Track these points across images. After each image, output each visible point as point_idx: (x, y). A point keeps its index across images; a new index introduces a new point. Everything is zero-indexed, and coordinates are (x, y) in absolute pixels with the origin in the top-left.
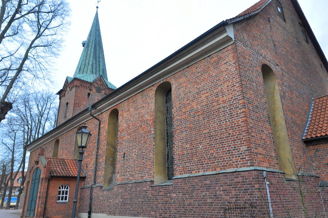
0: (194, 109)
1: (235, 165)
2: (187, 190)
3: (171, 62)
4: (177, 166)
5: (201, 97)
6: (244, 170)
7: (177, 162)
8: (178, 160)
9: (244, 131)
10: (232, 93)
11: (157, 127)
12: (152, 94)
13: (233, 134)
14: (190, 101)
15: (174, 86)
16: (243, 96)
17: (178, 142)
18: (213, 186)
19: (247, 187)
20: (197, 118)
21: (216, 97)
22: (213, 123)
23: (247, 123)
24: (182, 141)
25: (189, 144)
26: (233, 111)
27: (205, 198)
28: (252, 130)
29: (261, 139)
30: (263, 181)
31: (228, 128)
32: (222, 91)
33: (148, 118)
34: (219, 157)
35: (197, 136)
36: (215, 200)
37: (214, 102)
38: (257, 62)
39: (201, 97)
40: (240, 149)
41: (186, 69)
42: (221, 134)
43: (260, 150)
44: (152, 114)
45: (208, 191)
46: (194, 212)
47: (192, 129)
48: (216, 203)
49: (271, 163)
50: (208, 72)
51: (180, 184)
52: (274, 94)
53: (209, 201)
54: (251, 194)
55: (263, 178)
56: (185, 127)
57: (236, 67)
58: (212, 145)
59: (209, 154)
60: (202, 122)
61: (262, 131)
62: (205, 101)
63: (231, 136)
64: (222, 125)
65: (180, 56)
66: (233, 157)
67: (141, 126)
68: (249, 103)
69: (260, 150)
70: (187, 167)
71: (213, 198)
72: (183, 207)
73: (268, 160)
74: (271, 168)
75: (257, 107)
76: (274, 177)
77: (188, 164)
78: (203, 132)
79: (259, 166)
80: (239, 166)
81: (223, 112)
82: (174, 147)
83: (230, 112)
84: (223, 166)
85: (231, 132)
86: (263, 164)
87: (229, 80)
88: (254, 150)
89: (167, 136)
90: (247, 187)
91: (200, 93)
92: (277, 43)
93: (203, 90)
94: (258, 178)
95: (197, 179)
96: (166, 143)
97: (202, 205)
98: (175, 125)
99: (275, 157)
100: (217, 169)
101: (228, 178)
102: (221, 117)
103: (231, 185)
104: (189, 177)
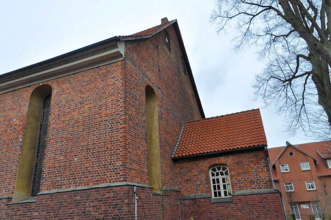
0: (75, 119)
1: (109, 180)
3: (55, 64)
5: (84, 107)
6: (117, 185)
7: (46, 175)
8: (48, 173)
9: (122, 146)
10: (115, 108)
11: (27, 135)
12: (27, 96)
13: (111, 148)
14: (71, 110)
15: (55, 91)
16: (125, 112)
17: (51, 153)
19: (117, 202)
20: (76, 129)
21: (99, 110)
22: (92, 136)
23: (125, 139)
24: (56, 152)
25: (63, 155)
26: (114, 125)
27: (72, 216)
28: (129, 145)
29: (137, 155)
30: (132, 196)
31: (107, 142)
32: (106, 104)
33: (18, 122)
34: (94, 171)
37: (96, 114)
38: (143, 82)
39: (84, 107)
41: (72, 76)
42: (99, 148)
43: (135, 166)
44: (23, 118)
45: (77, 208)
47: (69, 140)
49: (142, 178)
50: (94, 83)
51: (46, 201)
54: (120, 210)
55: (133, 193)
56: (62, 137)
57: (122, 83)
58: (89, 158)
59: (83, 168)
60: (82, 134)
61: (138, 147)
62: (88, 112)
63: (109, 151)
65: (67, 60)
66: (108, 172)
67: (6, 131)
68: (130, 120)
69: (135, 166)
70: (56, 181)
73: (141, 176)
74: (142, 183)
76: (144, 192)
77: (58, 178)
78: (80, 144)
79: (131, 181)
80: (112, 181)
81: (104, 125)
82: (45, 158)
83: (111, 126)
84: (96, 181)
85: (109, 146)
86: (135, 179)
87: (114, 94)
88: (128, 166)
89: (39, 146)
90: (117, 202)
91: (83, 103)
92: (161, 69)
93: (87, 101)
94: (128, 193)
95: (67, 194)
96: (36, 153)
98: (51, 133)
99: (147, 173)
100: (90, 184)
101: (99, 194)
102: (101, 130)
103: (102, 201)
104: (57, 193)
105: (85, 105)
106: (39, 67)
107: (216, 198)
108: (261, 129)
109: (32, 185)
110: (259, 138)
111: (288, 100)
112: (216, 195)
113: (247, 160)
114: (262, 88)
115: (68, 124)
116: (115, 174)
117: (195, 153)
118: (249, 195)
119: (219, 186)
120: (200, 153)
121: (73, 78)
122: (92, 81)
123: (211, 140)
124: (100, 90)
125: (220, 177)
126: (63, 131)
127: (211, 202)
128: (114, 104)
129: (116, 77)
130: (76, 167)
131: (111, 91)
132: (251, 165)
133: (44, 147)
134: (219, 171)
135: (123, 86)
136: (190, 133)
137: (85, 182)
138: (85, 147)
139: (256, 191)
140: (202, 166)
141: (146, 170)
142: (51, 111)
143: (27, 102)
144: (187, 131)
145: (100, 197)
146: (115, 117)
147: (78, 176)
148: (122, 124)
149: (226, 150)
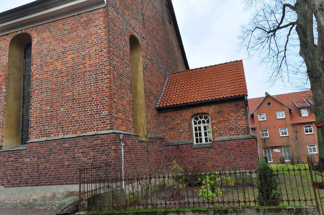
0: (58, 69)
2: (44, 154)
3: (32, 10)
4: (34, 129)
5: (67, 57)
6: (104, 133)
8: (35, 122)
9: (107, 97)
10: (99, 58)
11: (10, 85)
12: (6, 45)
13: (96, 98)
14: (54, 60)
17: (37, 104)
18: (72, 149)
19: (105, 148)
20: (60, 79)
21: (82, 60)
22: (77, 86)
23: (110, 89)
24: (41, 103)
25: (49, 106)
26: (99, 76)
27: (63, 161)
29: (122, 105)
30: (119, 143)
31: (92, 92)
32: (89, 54)
34: (81, 121)
35: (59, 98)
36: (72, 163)
39: (67, 57)
40: (102, 113)
41: (52, 24)
42: (84, 98)
43: (120, 115)
45: (66, 154)
46: (49, 176)
48: (73, 165)
50: (76, 31)
51: (36, 148)
52: (138, 64)
53: (66, 163)
55: (119, 140)
56: (46, 88)
57: (105, 31)
58: (75, 108)
59: (70, 117)
61: (124, 97)
62: (71, 62)
63: (95, 101)
64: (86, 89)
66: (94, 121)
71: (71, 160)
72: (37, 172)
73: (126, 125)
74: (127, 131)
75: (122, 75)
77: (46, 127)
78: (65, 95)
82: (31, 108)
83: (95, 77)
84: (84, 129)
85: (94, 96)
87: (97, 44)
88: (114, 115)
89: (24, 97)
90: (105, 148)
92: (145, 18)
93: (69, 51)
95: (56, 142)
96: (22, 104)
97: (58, 168)
98: (35, 84)
99: (132, 122)
100: (78, 132)
101: (87, 141)
102: (86, 80)
103: (90, 147)
105: (68, 55)
106: (15, 13)
107: (197, 144)
108: (243, 80)
110: (240, 89)
111: (271, 51)
112: (197, 141)
113: (228, 109)
114: (246, 40)
115: (52, 75)
116: (102, 123)
117: (178, 103)
118: (227, 141)
119: (200, 134)
120: (184, 103)
121: (53, 26)
122: (74, 30)
123: (194, 90)
124: (83, 39)
125: (202, 125)
126: (47, 81)
127: (193, 148)
128: (98, 54)
129: (98, 25)
130: (62, 116)
131: (94, 41)
132: (231, 114)
133: (29, 97)
134: (201, 120)
135: (106, 35)
136: (174, 84)
137: (72, 131)
138: (71, 98)
139: (234, 137)
140: (185, 115)
141: (131, 119)
142: (33, 61)
143: (6, 51)
144: (172, 82)
145: (88, 144)
146: (100, 67)
147: (65, 125)
148: (107, 74)
149: (209, 100)
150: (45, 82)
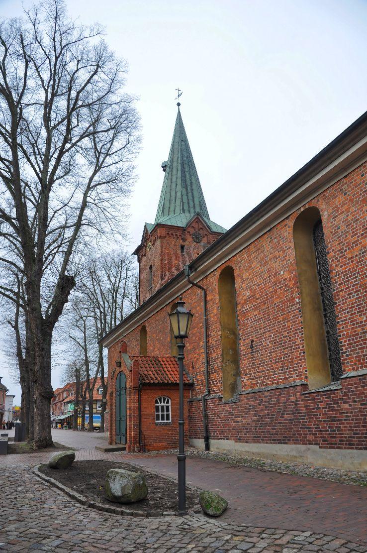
8: (348, 344)
11: (304, 290)
14: (358, 237)
17: (345, 313)
24: (352, 311)
33: (287, 276)
41: (344, 181)
51: (356, 387)
56: (355, 285)
65: (329, 159)
67: (276, 291)
82: (338, 322)
96: (323, 316)
98: (336, 282)
106: (315, 166)
109: (329, 364)
121: (346, 183)
126: (354, 274)
150: (351, 276)
